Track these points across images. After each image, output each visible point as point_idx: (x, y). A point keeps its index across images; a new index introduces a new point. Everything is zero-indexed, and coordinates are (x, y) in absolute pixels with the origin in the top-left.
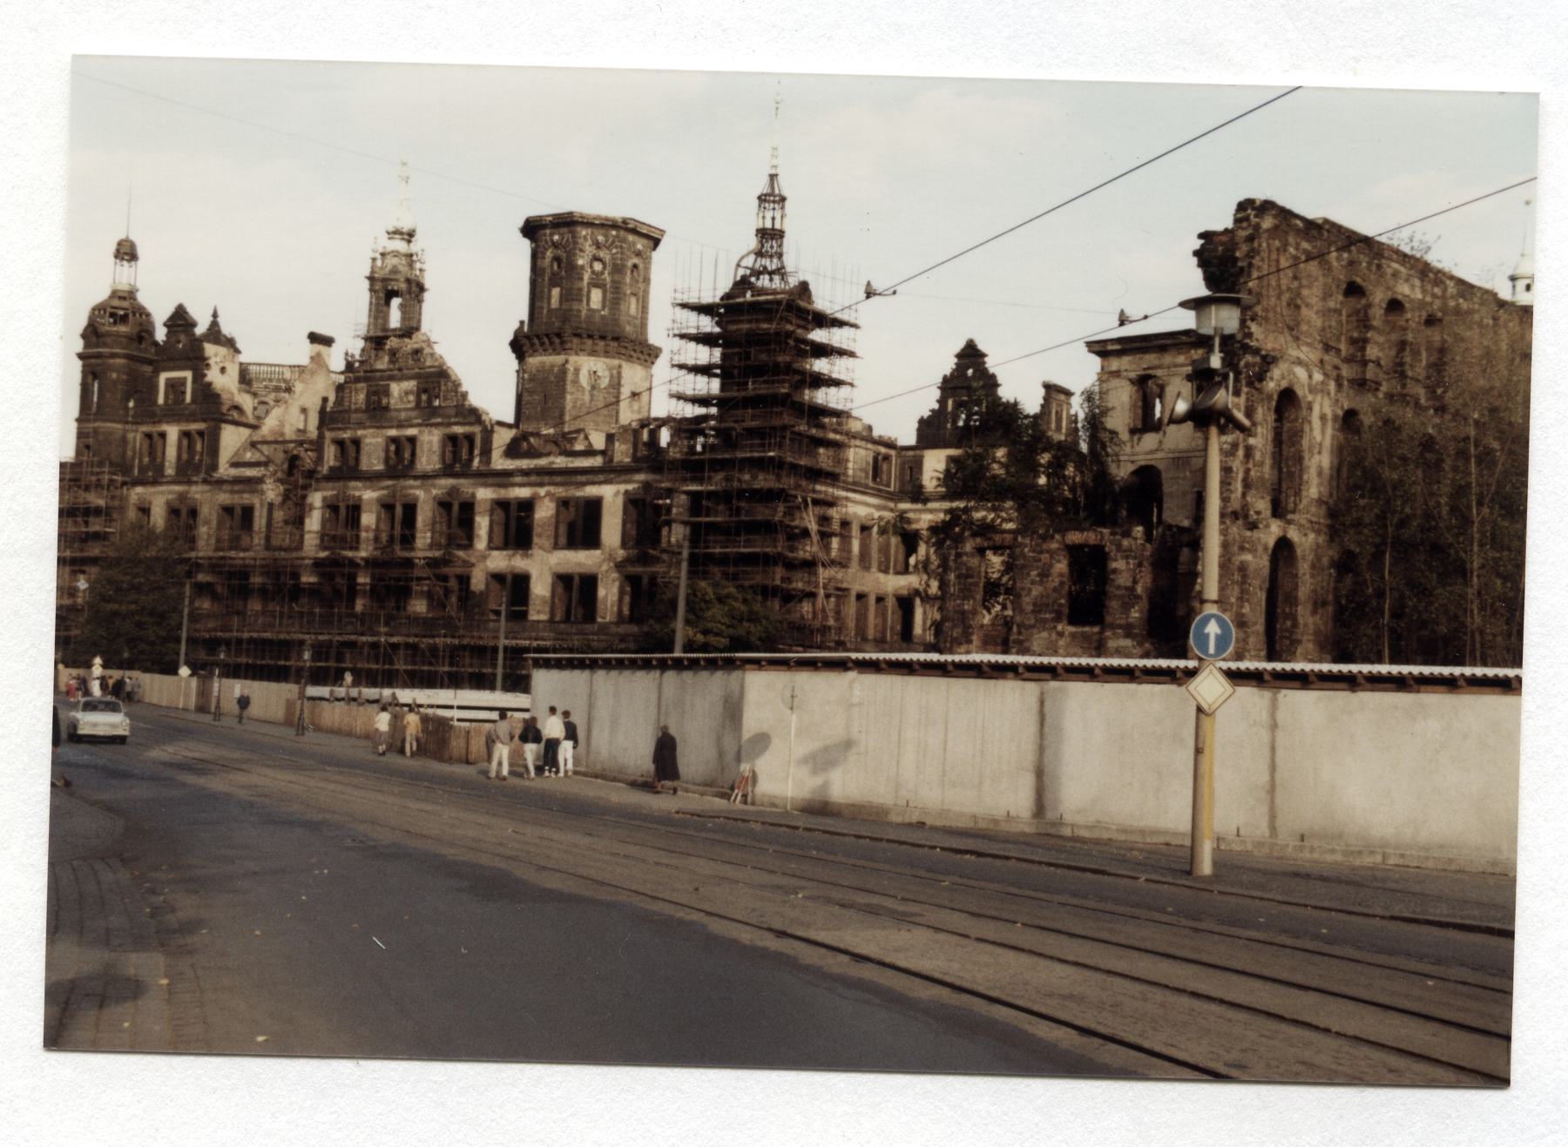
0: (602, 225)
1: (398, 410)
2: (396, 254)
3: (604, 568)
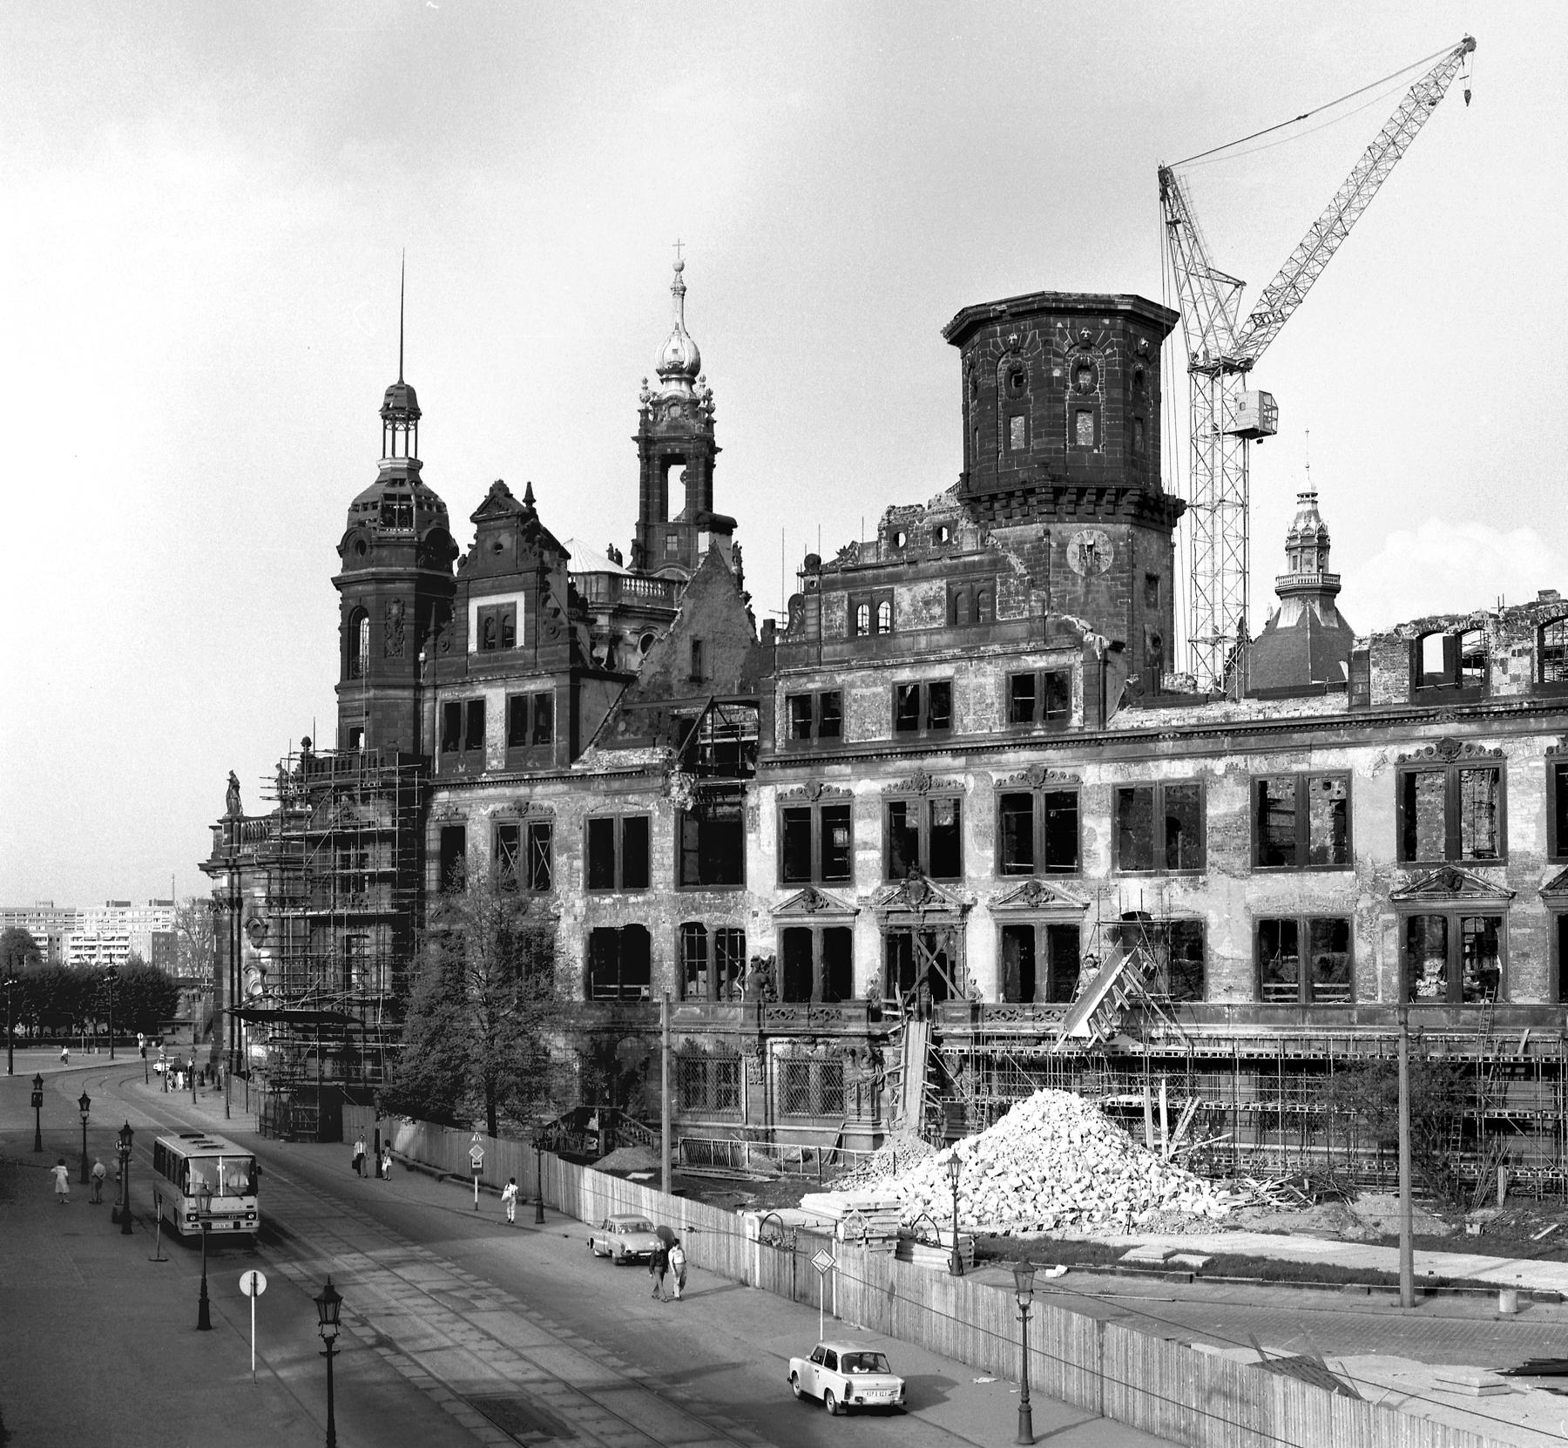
0: (1087, 312)
1: (913, 634)
2: (674, 401)
3: (1365, 902)
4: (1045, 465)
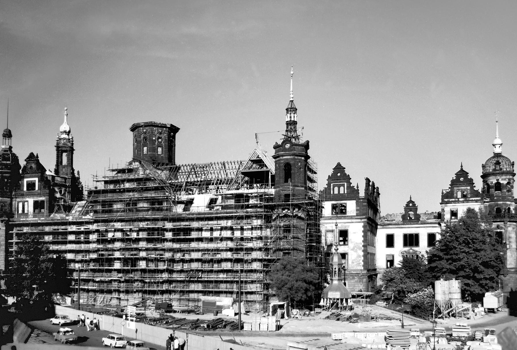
0: (161, 127)
4: (151, 158)
